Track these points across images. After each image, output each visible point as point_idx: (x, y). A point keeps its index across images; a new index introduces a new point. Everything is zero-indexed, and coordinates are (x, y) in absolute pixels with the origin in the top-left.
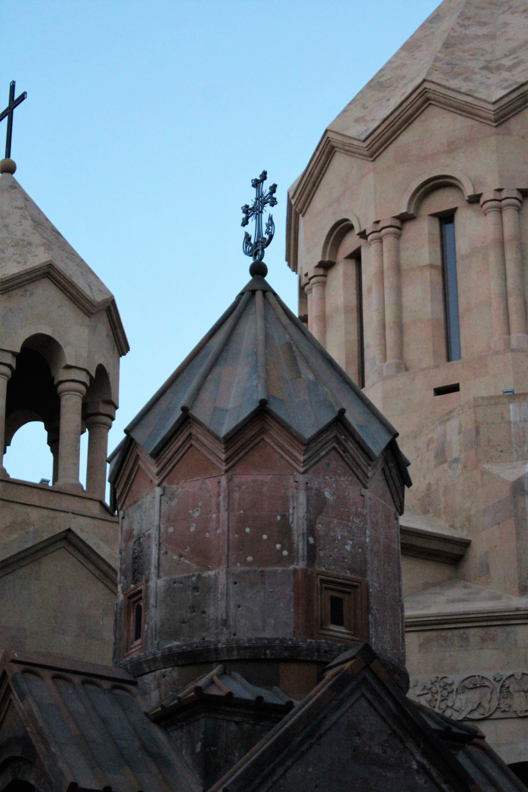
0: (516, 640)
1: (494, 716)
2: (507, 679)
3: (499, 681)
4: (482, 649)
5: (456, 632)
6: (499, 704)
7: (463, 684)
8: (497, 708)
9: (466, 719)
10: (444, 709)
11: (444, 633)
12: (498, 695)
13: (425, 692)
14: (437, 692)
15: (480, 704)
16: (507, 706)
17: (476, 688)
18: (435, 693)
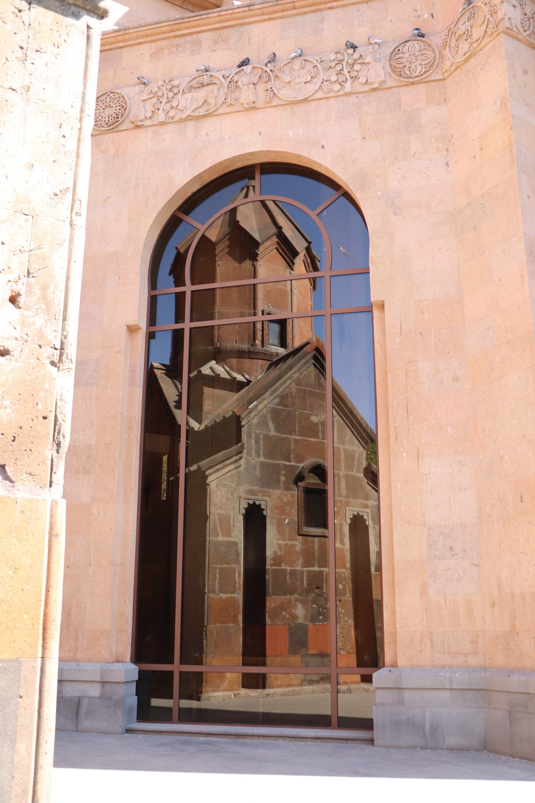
0: (249, 39)
1: (220, 111)
2: (235, 74)
3: (228, 77)
4: (213, 51)
5: (189, 38)
6: (225, 99)
7: (190, 84)
8: (223, 102)
9: (190, 118)
10: (168, 110)
11: (176, 41)
12: (226, 89)
13: (151, 96)
14: (163, 94)
15: (205, 101)
16: (233, 100)
17: (204, 86)
18: (161, 97)
